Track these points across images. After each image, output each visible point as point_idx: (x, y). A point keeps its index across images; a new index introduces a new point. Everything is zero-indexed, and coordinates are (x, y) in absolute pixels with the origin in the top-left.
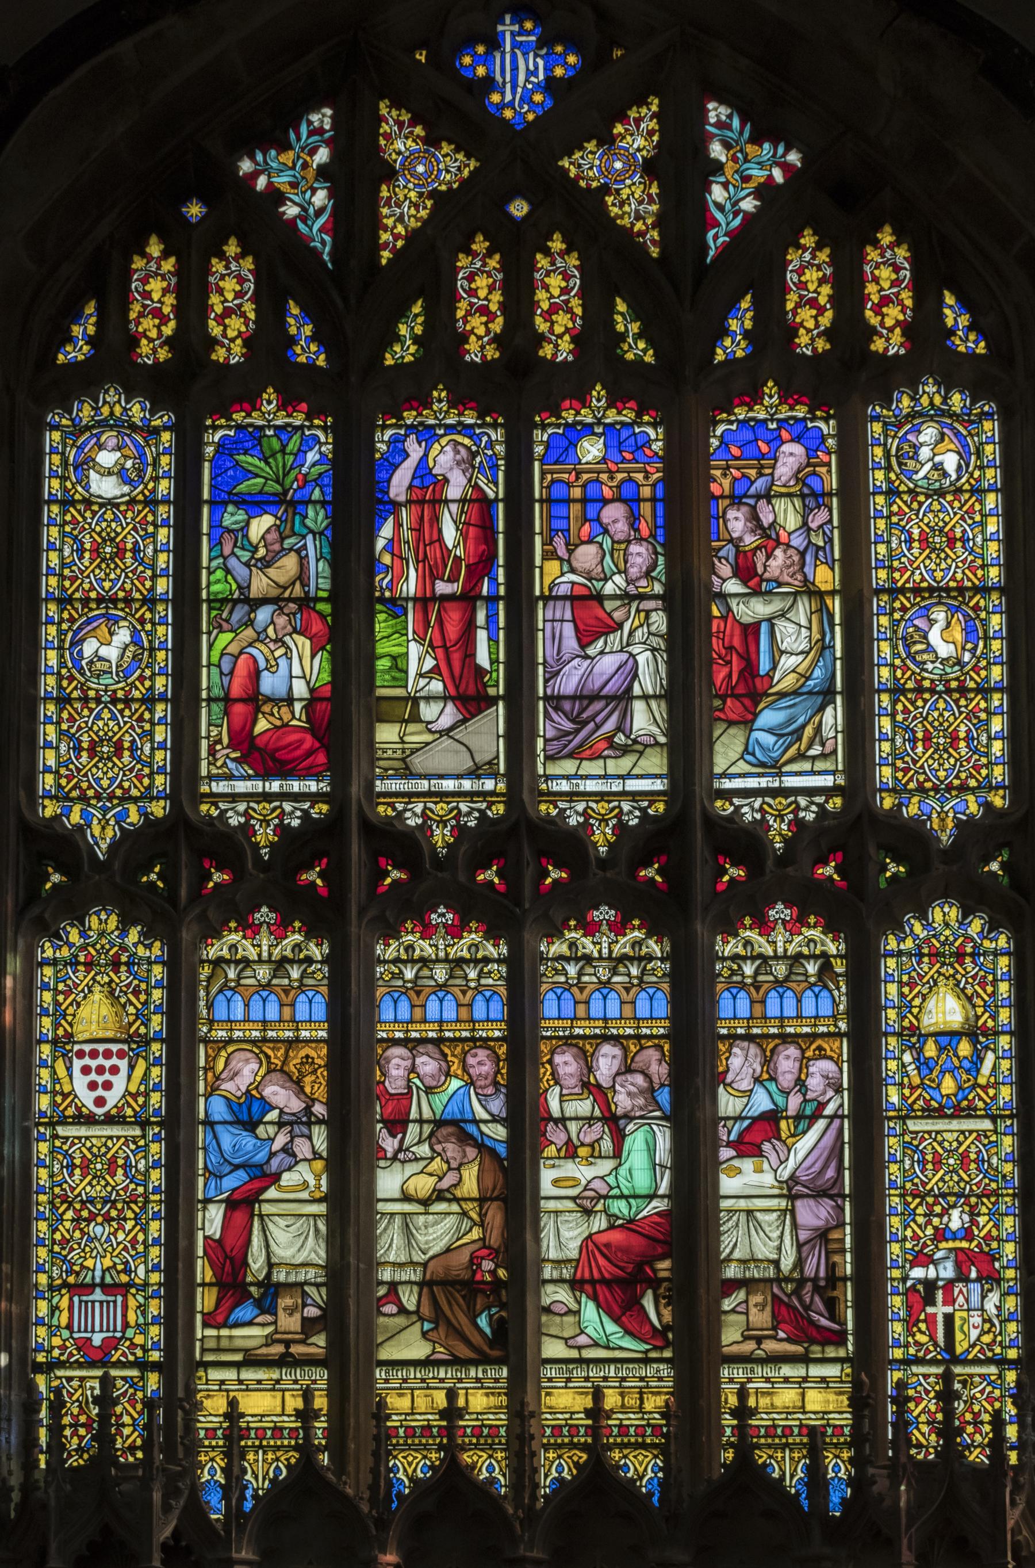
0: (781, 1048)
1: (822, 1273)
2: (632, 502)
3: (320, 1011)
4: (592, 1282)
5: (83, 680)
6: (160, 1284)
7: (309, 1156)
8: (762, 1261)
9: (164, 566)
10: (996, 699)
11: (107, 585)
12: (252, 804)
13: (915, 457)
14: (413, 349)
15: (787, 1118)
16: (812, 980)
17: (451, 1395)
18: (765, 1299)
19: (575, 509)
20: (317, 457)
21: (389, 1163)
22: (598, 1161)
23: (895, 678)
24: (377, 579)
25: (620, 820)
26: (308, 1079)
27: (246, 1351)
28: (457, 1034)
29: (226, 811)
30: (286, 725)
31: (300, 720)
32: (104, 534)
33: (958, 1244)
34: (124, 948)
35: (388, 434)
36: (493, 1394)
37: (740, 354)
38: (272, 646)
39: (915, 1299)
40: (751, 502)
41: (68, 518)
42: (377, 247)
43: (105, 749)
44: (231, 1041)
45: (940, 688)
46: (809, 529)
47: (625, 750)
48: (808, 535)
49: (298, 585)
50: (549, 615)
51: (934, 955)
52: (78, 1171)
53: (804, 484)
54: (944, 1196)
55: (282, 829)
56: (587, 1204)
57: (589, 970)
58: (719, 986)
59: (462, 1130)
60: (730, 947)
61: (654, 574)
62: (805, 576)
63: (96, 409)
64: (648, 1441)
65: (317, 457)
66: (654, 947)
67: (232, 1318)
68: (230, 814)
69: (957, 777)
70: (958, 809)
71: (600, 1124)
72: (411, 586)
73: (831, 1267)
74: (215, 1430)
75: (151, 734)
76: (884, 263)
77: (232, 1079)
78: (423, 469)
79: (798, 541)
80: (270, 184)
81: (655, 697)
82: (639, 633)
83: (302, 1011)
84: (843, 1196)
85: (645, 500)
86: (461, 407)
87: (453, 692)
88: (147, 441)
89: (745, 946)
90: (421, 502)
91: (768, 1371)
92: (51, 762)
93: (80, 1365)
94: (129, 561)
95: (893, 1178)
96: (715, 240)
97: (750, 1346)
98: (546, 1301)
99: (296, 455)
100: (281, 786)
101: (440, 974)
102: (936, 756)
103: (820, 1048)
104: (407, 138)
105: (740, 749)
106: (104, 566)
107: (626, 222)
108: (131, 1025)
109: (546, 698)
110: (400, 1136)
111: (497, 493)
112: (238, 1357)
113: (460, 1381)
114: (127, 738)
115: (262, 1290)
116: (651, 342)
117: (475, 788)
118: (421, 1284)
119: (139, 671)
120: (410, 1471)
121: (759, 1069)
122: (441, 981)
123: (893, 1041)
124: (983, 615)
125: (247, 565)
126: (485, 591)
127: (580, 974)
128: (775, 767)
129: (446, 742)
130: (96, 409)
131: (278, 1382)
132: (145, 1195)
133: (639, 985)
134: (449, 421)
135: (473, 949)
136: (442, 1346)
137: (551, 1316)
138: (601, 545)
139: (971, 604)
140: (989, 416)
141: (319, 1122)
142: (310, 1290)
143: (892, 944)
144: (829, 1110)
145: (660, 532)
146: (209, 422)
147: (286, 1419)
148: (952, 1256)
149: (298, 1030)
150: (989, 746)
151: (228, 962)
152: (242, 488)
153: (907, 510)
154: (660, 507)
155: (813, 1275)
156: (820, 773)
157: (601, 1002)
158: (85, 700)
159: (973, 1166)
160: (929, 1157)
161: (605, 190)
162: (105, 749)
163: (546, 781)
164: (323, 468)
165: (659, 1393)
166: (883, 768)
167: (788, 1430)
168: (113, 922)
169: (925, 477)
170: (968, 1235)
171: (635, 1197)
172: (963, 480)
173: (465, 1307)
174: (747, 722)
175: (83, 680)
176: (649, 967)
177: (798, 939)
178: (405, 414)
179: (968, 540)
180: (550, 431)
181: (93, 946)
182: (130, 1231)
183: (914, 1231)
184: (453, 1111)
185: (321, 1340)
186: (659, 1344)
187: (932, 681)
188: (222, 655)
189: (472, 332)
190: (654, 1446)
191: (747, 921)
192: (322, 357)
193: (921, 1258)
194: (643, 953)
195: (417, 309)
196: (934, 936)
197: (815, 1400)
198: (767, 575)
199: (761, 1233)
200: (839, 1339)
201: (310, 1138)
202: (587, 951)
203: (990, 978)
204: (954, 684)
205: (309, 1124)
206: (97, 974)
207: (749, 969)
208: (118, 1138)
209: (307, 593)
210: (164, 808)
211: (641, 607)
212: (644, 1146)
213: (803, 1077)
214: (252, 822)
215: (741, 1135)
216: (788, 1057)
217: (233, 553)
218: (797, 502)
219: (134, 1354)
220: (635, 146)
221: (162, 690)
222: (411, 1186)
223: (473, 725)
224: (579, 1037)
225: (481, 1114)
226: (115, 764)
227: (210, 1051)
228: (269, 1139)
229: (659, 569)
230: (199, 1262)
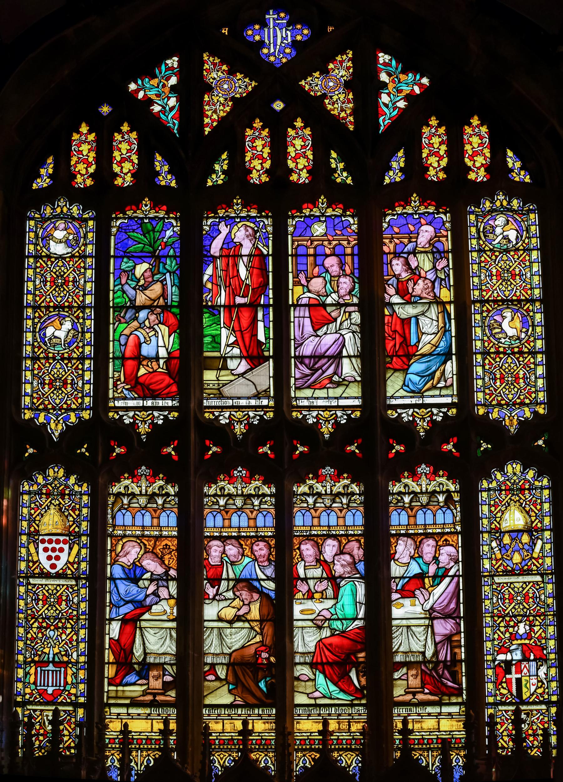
0: (425, 540)
1: (449, 659)
2: (341, 257)
3: (173, 521)
4: (322, 664)
6: (85, 662)
7: (167, 597)
9: (90, 289)
10: (539, 357)
11: (59, 299)
12: (137, 413)
13: (493, 232)
14: (222, 177)
15: (429, 577)
16: (442, 504)
17: (245, 723)
18: (417, 673)
19: (311, 259)
20: (172, 233)
21: (210, 601)
22: (325, 600)
23: (484, 346)
24: (204, 296)
25: (336, 421)
26: (167, 557)
27: (131, 698)
28: (248, 534)
29: (123, 416)
30: (155, 371)
31: (162, 369)
32: (57, 273)
33: (523, 641)
34: (67, 486)
35: (210, 221)
36: (267, 722)
37: (398, 179)
38: (147, 330)
39: (499, 670)
40: (405, 256)
41: (38, 265)
42: (202, 126)
43: (58, 384)
44: (125, 536)
45: (509, 352)
46: (437, 270)
47: (338, 384)
48: (436, 273)
49: (161, 299)
50: (297, 314)
52: (41, 602)
53: (434, 247)
54: (515, 616)
55: (153, 425)
56: (319, 623)
57: (320, 500)
58: (391, 509)
59: (252, 584)
60: (397, 488)
63: (54, 209)
64: (353, 747)
65: (172, 233)
66: (355, 488)
69: (519, 398)
70: (519, 415)
71: (326, 581)
72: (222, 299)
73: (453, 655)
74: (114, 739)
75: (83, 376)
76: (474, 135)
78: (229, 240)
79: (431, 276)
80: (145, 95)
81: (354, 356)
83: (163, 521)
84: (460, 618)
85: (348, 255)
86: (249, 208)
87: (245, 354)
88: (81, 226)
89: (405, 487)
90: (228, 256)
91: (419, 710)
92: (29, 390)
93: (40, 704)
94: (71, 287)
95: (487, 607)
96: (384, 122)
97: (409, 697)
98: (297, 674)
100: (153, 403)
101: (239, 502)
102: (507, 387)
103: (446, 540)
104: (218, 71)
105: (402, 383)
106: (57, 289)
107: (335, 112)
108: (70, 526)
109: (295, 357)
110: (217, 587)
111: (268, 252)
112: (128, 702)
113: (250, 715)
114: (70, 378)
118: (228, 665)
119: (76, 344)
120: (222, 762)
121: (413, 552)
122: (239, 506)
123: (486, 536)
125: (134, 288)
126: (262, 302)
127: (315, 502)
128: (420, 393)
129: (241, 380)
130: (54, 209)
131: (149, 715)
132: (78, 616)
133: (347, 508)
134: (242, 215)
135: (257, 489)
136: (239, 697)
138: (324, 278)
139: (525, 308)
140: (533, 211)
141: (173, 579)
142: (168, 667)
143: (485, 484)
144: (451, 573)
146: (114, 216)
147: (153, 734)
148: (520, 648)
149: (161, 531)
150: (536, 382)
151: (124, 495)
153: (489, 260)
154: (356, 259)
156: (444, 396)
157: (327, 517)
158: (47, 358)
159: (531, 600)
160: (507, 596)
161: (324, 96)
162: (58, 384)
163: (296, 400)
165: (359, 722)
166: (478, 393)
167: (430, 741)
168: (61, 472)
169: (499, 243)
170: (529, 637)
171: (346, 619)
172: (520, 244)
173: (252, 677)
174: (405, 370)
176: (352, 499)
177: (433, 483)
179: (523, 275)
180: (297, 219)
181: (51, 485)
182: (69, 634)
183: (499, 635)
184: (246, 574)
185: (173, 693)
187: (504, 348)
188: (121, 335)
189: (254, 168)
190: (356, 749)
191: (406, 474)
192: (174, 181)
193: (503, 649)
194: (349, 491)
195: (224, 156)
196: (508, 480)
197: (446, 725)
198: (414, 294)
200: (459, 693)
202: (319, 491)
203: (539, 501)
204: (516, 350)
205: (167, 580)
207: (407, 499)
208: (63, 585)
210: (90, 414)
211: (346, 310)
212: (350, 593)
213: (437, 555)
214: (137, 422)
215: (403, 586)
216: (429, 545)
217: (127, 283)
218: (430, 256)
219: (70, 699)
220: (340, 74)
221: (88, 353)
222: (222, 614)
223: (256, 371)
224: (314, 535)
226: (63, 392)
227: (113, 541)
228: (145, 588)
229: (356, 290)
230: (107, 651)
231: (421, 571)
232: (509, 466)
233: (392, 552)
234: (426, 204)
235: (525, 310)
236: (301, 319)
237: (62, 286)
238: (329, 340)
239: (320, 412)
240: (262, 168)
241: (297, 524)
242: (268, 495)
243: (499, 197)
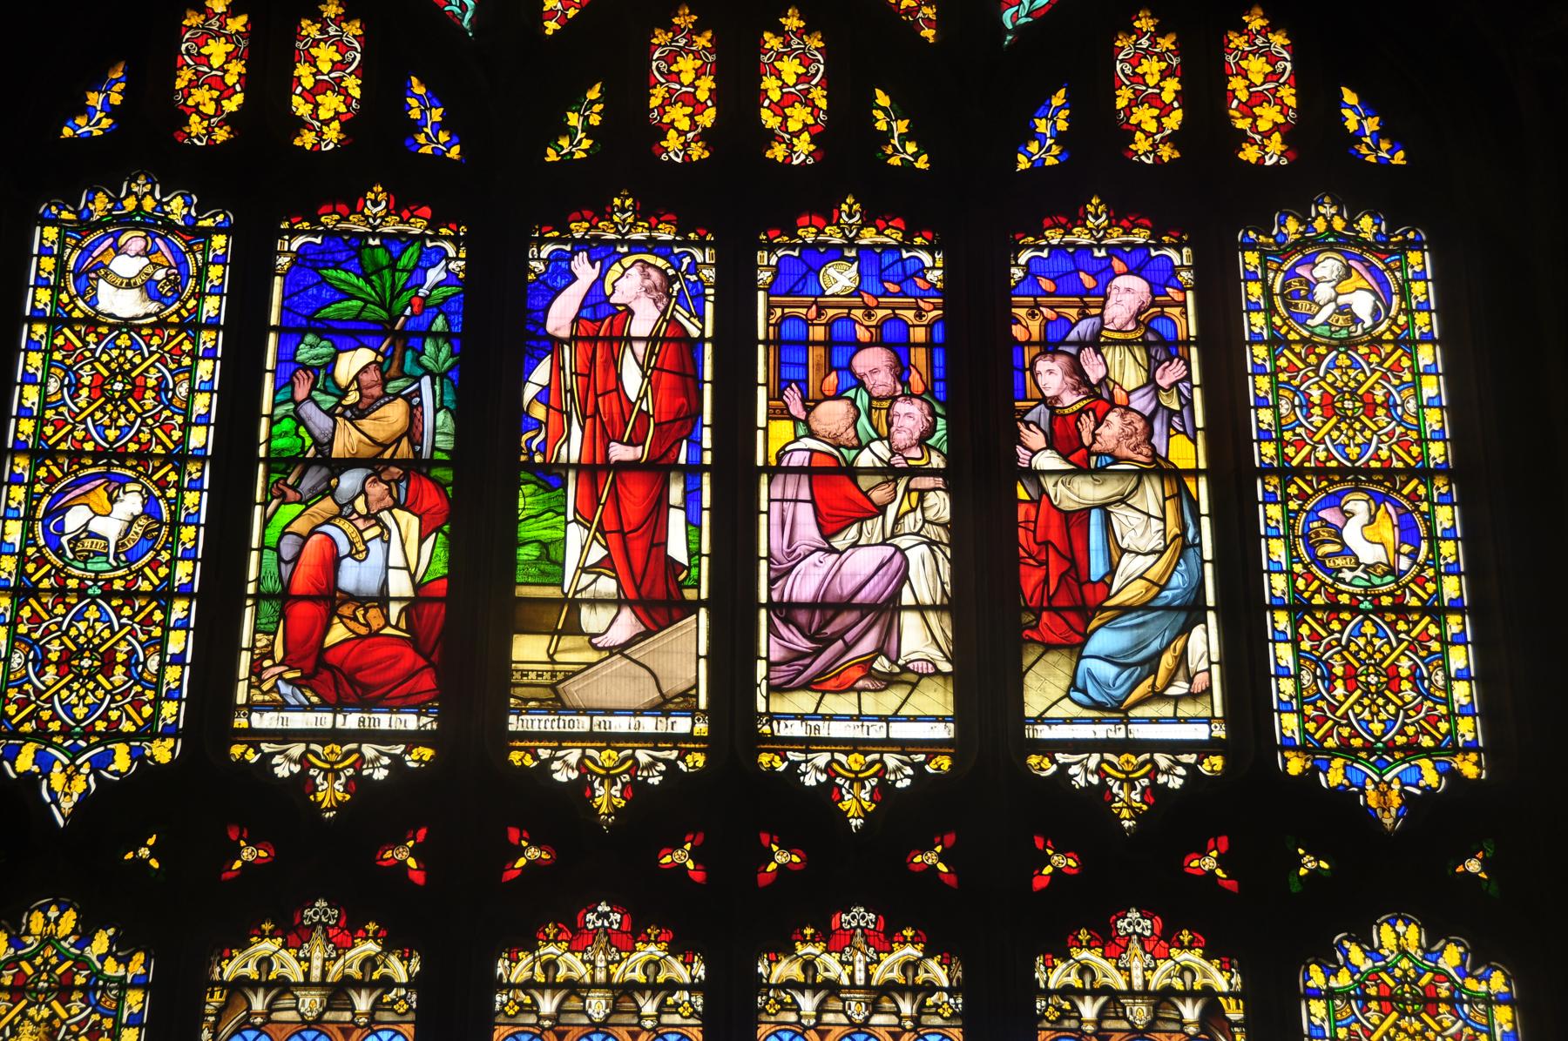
5: (60, 564)
9: (203, 411)
10: (1454, 623)
11: (112, 434)
13: (1310, 296)
14: (586, 144)
19: (816, 355)
20: (443, 276)
24: (525, 438)
25: (882, 781)
29: (272, 755)
30: (377, 634)
31: (396, 627)
34: (82, 963)
35: (546, 250)
37: (1051, 161)
38: (360, 524)
40: (1072, 350)
43: (86, 663)
45: (1366, 605)
46: (1157, 388)
47: (889, 681)
48: (1156, 396)
49: (405, 442)
50: (776, 494)
51: (1389, 1000)
55: (359, 784)
60: (1058, 975)
61: (930, 442)
62: (1153, 448)
63: (117, 201)
65: (443, 276)
66: (937, 972)
68: (277, 760)
69: (1402, 732)
72: (573, 449)
75: (163, 642)
78: (596, 301)
79: (1141, 403)
81: (934, 607)
82: (909, 519)
86: (653, 220)
87: (632, 594)
89: (1081, 974)
90: (593, 339)
94: (149, 404)
99: (411, 272)
100: (362, 721)
102: (1366, 701)
105: (1065, 682)
106: (109, 408)
109: (771, 606)
111: (703, 331)
114: (123, 647)
116: (923, 148)
117: (662, 729)
119: (151, 554)
124: (1424, 507)
125: (330, 413)
126: (682, 460)
127: (821, 1010)
128: (1117, 710)
129: (618, 663)
133: (914, 1030)
135: (651, 968)
138: (853, 402)
139: (1405, 491)
140: (1416, 245)
143: (1317, 978)
145: (939, 386)
150: (1448, 689)
151: (254, 985)
152: (329, 312)
153: (1301, 365)
154: (939, 359)
156: (1186, 720)
162: (86, 663)
164: (454, 290)
166: (1284, 716)
168: (69, 920)
169: (1326, 323)
172: (1383, 328)
174: (1075, 647)
175: (60, 564)
176: (929, 1002)
177: (1165, 966)
178: (573, 226)
179: (1395, 405)
180: (780, 253)
181: (30, 959)
187: (1353, 595)
188: (283, 534)
189: (672, 124)
191: (1084, 936)
194: (919, 981)
198: (1096, 447)
202: (832, 975)
204: (1386, 601)
206: (29, 1005)
209: (418, 454)
210: (173, 750)
211: (913, 485)
214: (312, 772)
218: (1140, 353)
221: (185, 580)
229: (938, 435)
232: (1386, 928)
234: (1125, 223)
235: (1407, 497)
236: (789, 506)
237: (123, 399)
238: (863, 562)
239: (838, 756)
240: (694, 125)
242: (683, 987)
243: (1321, 209)
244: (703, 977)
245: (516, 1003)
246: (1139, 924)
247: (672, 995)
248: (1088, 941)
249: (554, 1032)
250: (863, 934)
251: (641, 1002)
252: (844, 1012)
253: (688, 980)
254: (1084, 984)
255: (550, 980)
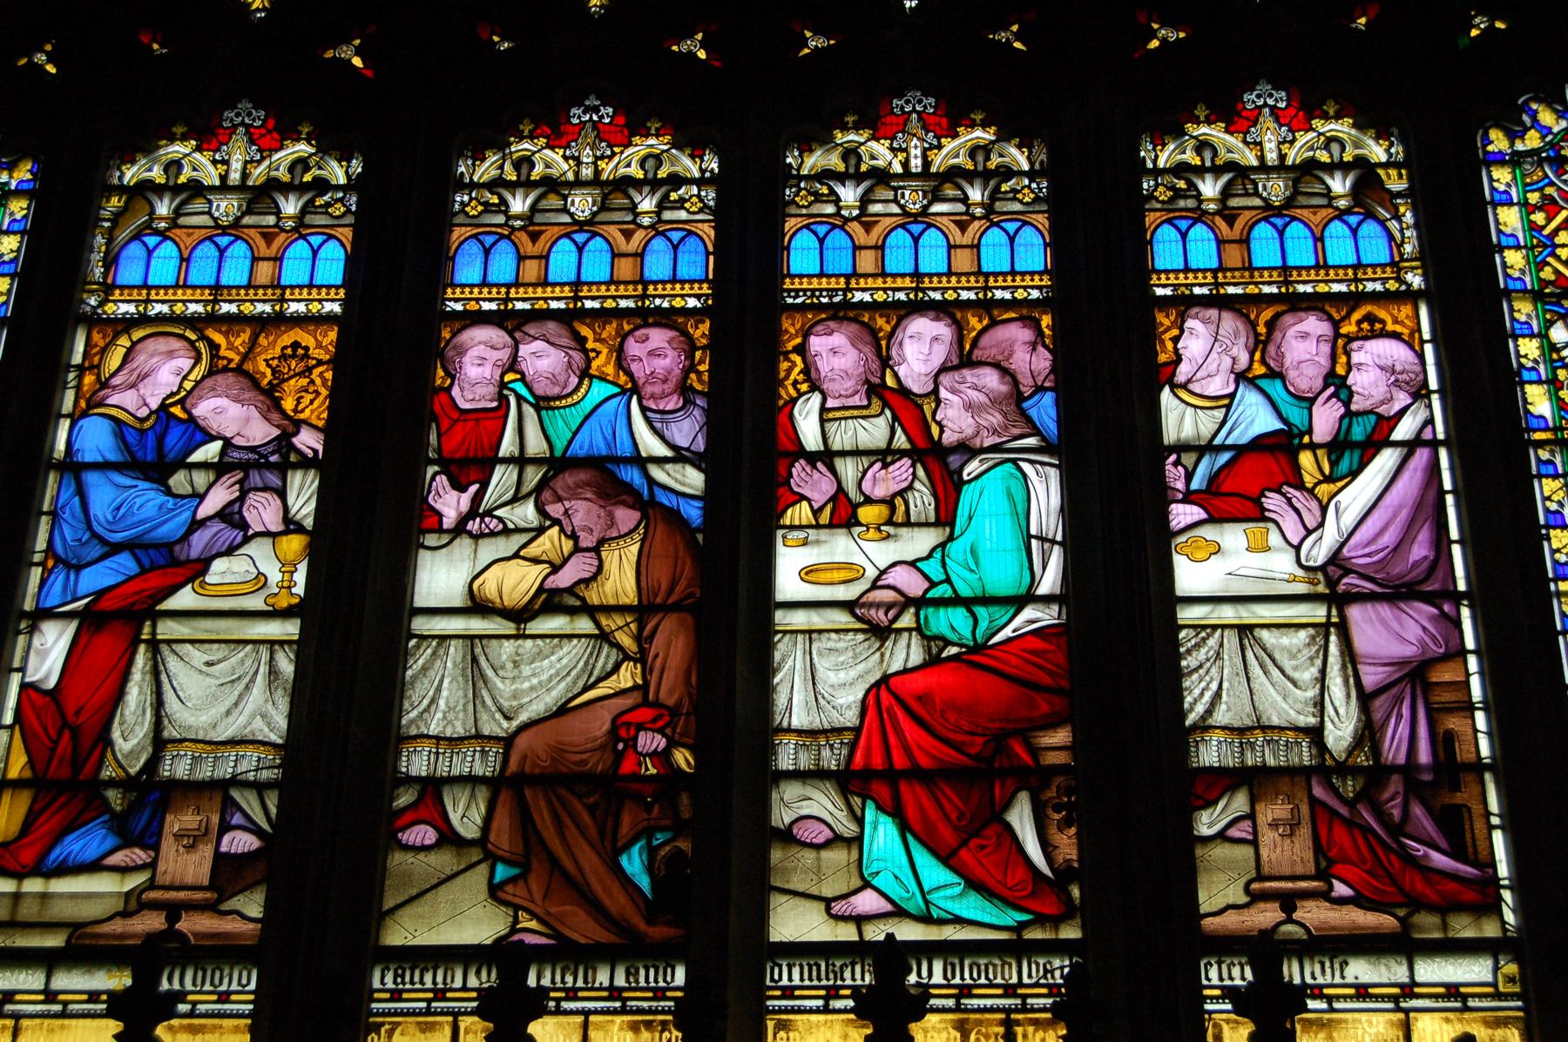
0: (1288, 319)
1: (1424, 756)
4: (891, 776)
7: (275, 524)
8: (1281, 729)
15: (1313, 447)
16: (1342, 203)
21: (445, 539)
22: (903, 531)
27: (75, 927)
28: (610, 304)
44: (143, 320)
56: (880, 616)
58: (1150, 218)
67: (56, 854)
71: (906, 462)
77: (133, 386)
83: (295, 269)
97: (1266, 916)
98: (782, 816)
101: (582, 204)
103: (1370, 318)
110: (474, 488)
112: (55, 941)
115: (133, 796)
118: (494, 784)
123: (1524, 309)
127: (865, 201)
133: (985, 217)
135: (650, 163)
136: (534, 915)
137: (794, 849)
141: (305, 463)
142: (248, 801)
143: (1498, 142)
144: (1403, 431)
151: (159, 190)
155: (1401, 759)
171: (987, 601)
173: (593, 832)
176: (1004, 188)
177: (1303, 138)
184: (592, 441)
185: (253, 905)
186: (1050, 909)
194: (992, 165)
199: (1275, 673)
201: (282, 494)
202: (880, 163)
205: (283, 469)
207: (1209, 188)
212: (1005, 507)
213: (1340, 370)
215: (1213, 479)
216: (1305, 336)
222: (489, 586)
225: (651, 445)
227: (97, 337)
231: (1278, 425)
233: (1162, 358)
241: (795, 268)
242: (692, 181)
244: (716, 171)
245: (481, 204)
246: (1271, 96)
247: (676, 190)
248: (1206, 116)
249: (527, 232)
250: (920, 118)
251: (637, 198)
252: (895, 201)
253: (697, 175)
254: (1203, 160)
255: (523, 178)
